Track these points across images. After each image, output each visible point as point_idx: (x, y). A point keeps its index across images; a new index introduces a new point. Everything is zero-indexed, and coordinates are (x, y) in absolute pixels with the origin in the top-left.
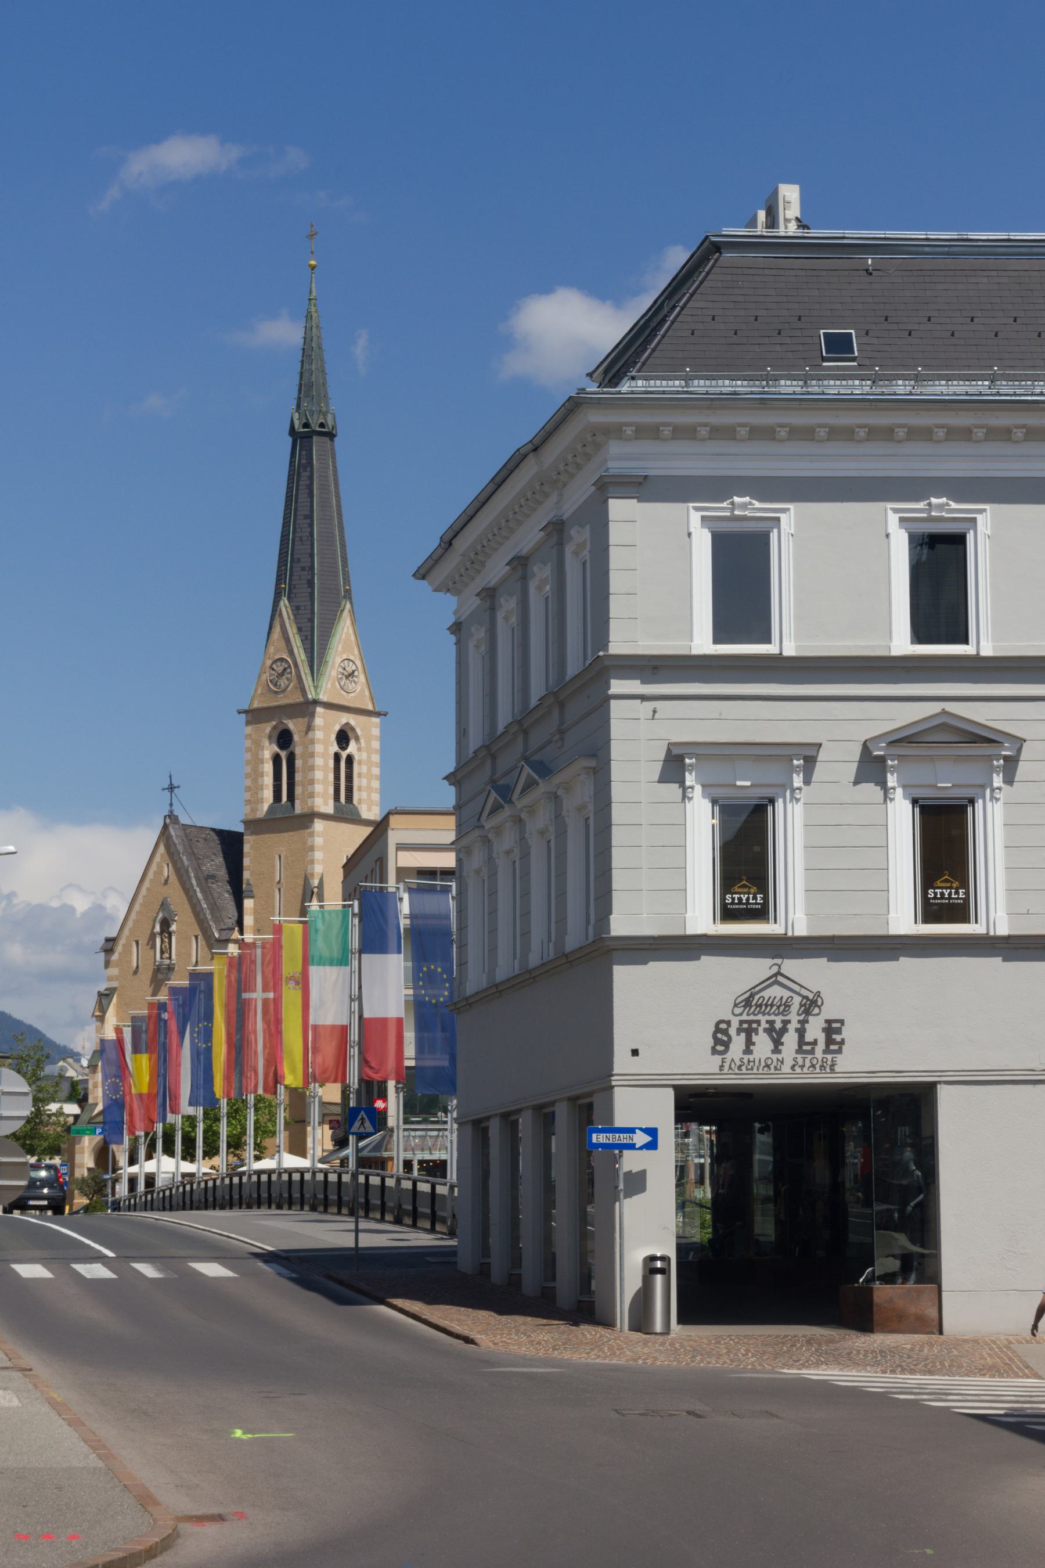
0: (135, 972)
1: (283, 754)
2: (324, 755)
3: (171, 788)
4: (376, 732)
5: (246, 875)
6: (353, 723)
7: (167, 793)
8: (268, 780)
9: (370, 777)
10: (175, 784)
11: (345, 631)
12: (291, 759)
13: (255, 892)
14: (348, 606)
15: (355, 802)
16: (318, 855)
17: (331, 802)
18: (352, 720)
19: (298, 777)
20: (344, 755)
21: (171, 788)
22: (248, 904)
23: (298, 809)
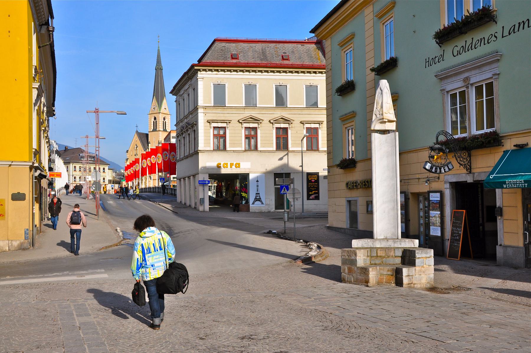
0: (132, 155)
1: (155, 121)
2: (161, 121)
3: (137, 126)
4: (170, 118)
5: (149, 140)
6: (166, 116)
7: (136, 127)
8: (153, 125)
9: (168, 125)
10: (137, 126)
11: (165, 101)
12: (156, 122)
13: (151, 143)
14: (165, 97)
15: (166, 129)
16: (160, 137)
17: (163, 129)
18: (166, 116)
19: (157, 125)
20: (164, 121)
21: (137, 126)
22: (149, 145)
23: (157, 130)
